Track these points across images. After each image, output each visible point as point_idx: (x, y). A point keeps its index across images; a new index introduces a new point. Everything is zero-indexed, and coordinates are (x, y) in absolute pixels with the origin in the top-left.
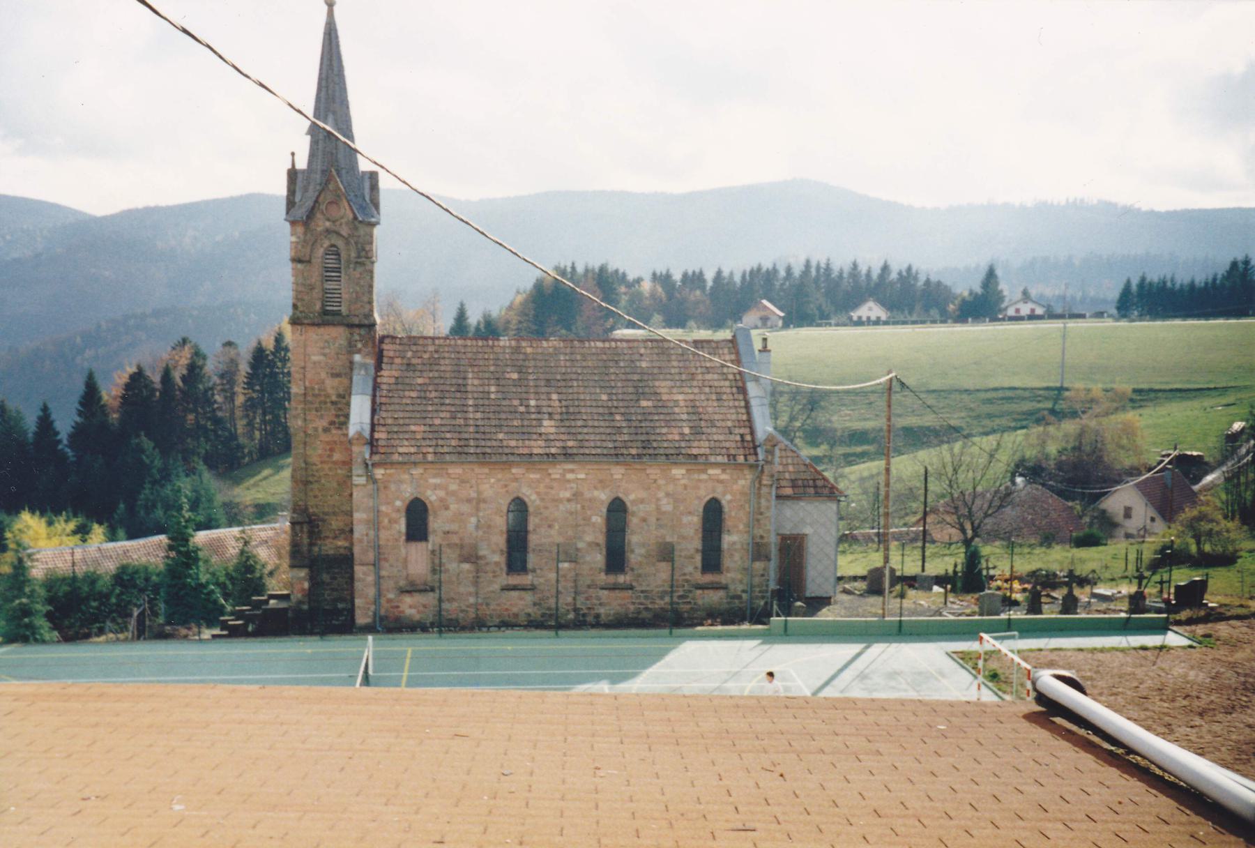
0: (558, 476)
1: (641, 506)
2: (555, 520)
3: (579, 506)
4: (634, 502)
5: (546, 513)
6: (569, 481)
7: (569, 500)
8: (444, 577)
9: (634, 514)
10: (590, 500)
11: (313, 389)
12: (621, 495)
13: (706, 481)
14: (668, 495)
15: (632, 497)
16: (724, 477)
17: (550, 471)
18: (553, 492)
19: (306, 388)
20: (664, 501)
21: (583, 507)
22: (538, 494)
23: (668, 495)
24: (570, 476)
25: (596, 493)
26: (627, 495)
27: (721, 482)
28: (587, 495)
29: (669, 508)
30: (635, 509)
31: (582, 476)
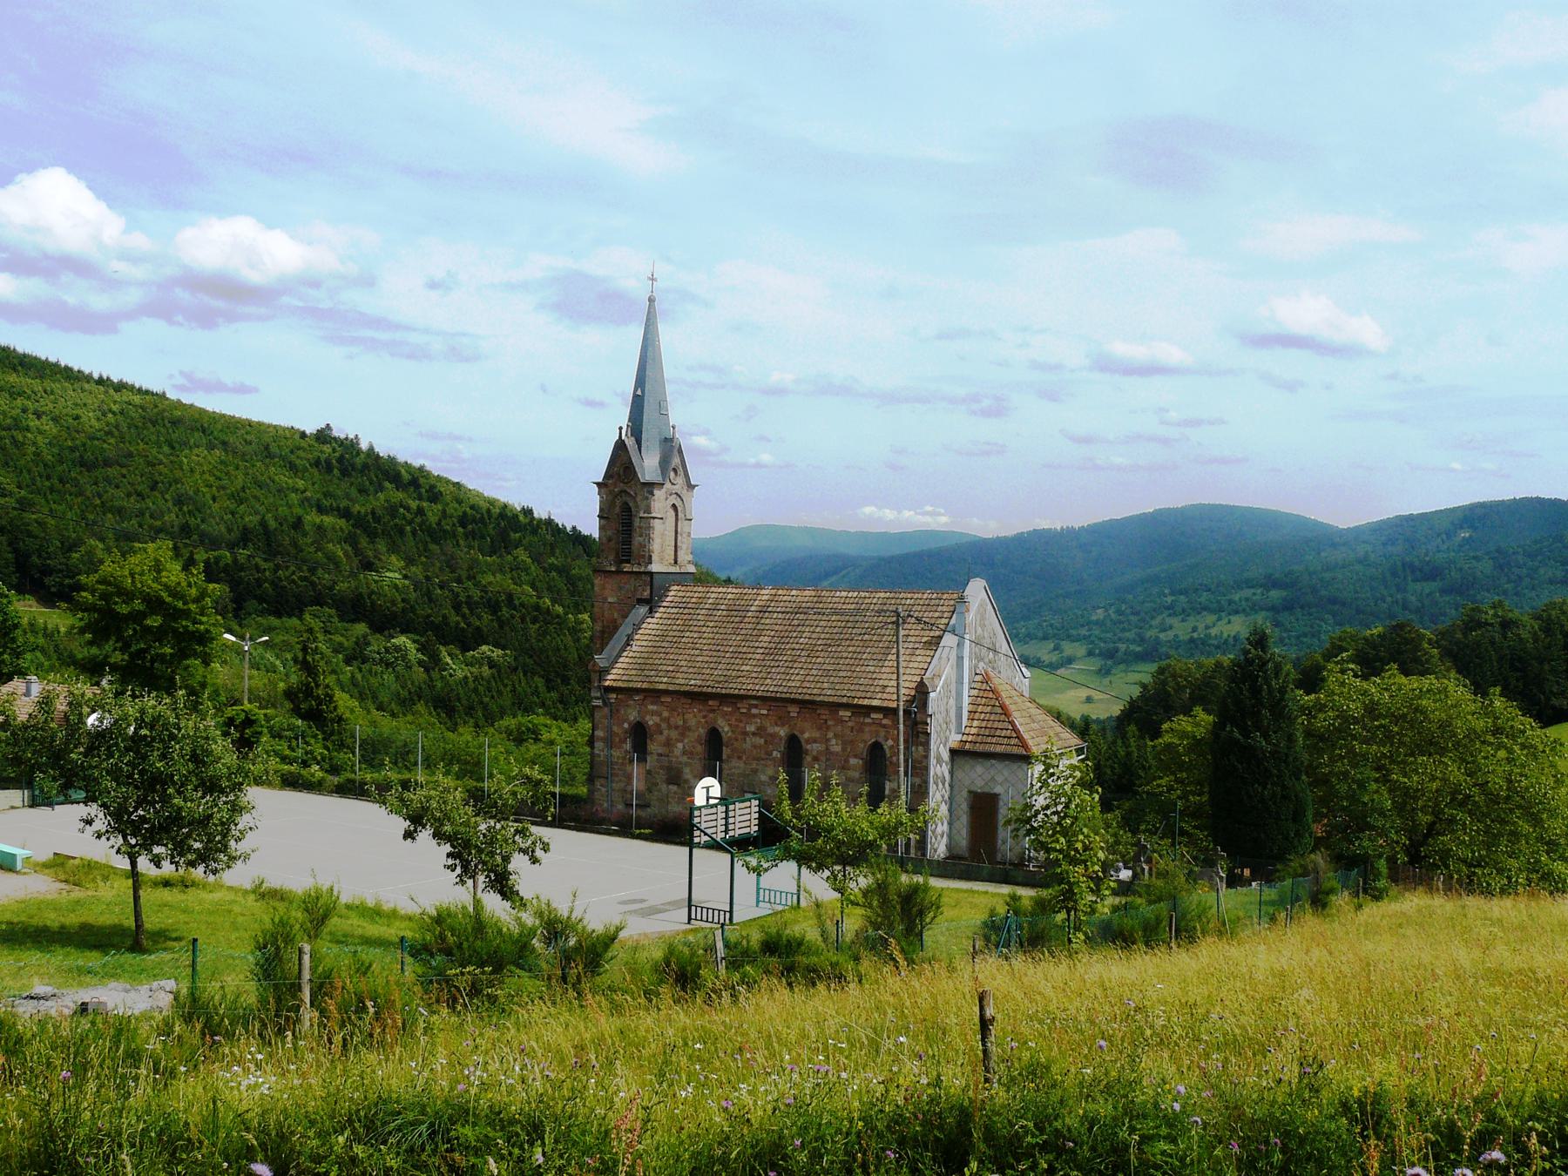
0: (745, 711)
1: (815, 745)
2: (744, 752)
3: (763, 740)
4: (808, 741)
5: (736, 744)
6: (754, 716)
7: (754, 734)
8: (1096, 1081)
9: (807, 752)
10: (771, 735)
11: (609, 627)
12: (796, 733)
13: (869, 724)
14: (836, 736)
15: (806, 735)
16: (885, 722)
17: (739, 705)
18: (741, 725)
19: (603, 627)
20: (834, 742)
21: (766, 742)
22: (730, 725)
23: (836, 736)
24: (754, 711)
25: (777, 729)
26: (803, 732)
27: (884, 726)
28: (771, 730)
29: (837, 749)
30: (809, 747)
31: (765, 712)
